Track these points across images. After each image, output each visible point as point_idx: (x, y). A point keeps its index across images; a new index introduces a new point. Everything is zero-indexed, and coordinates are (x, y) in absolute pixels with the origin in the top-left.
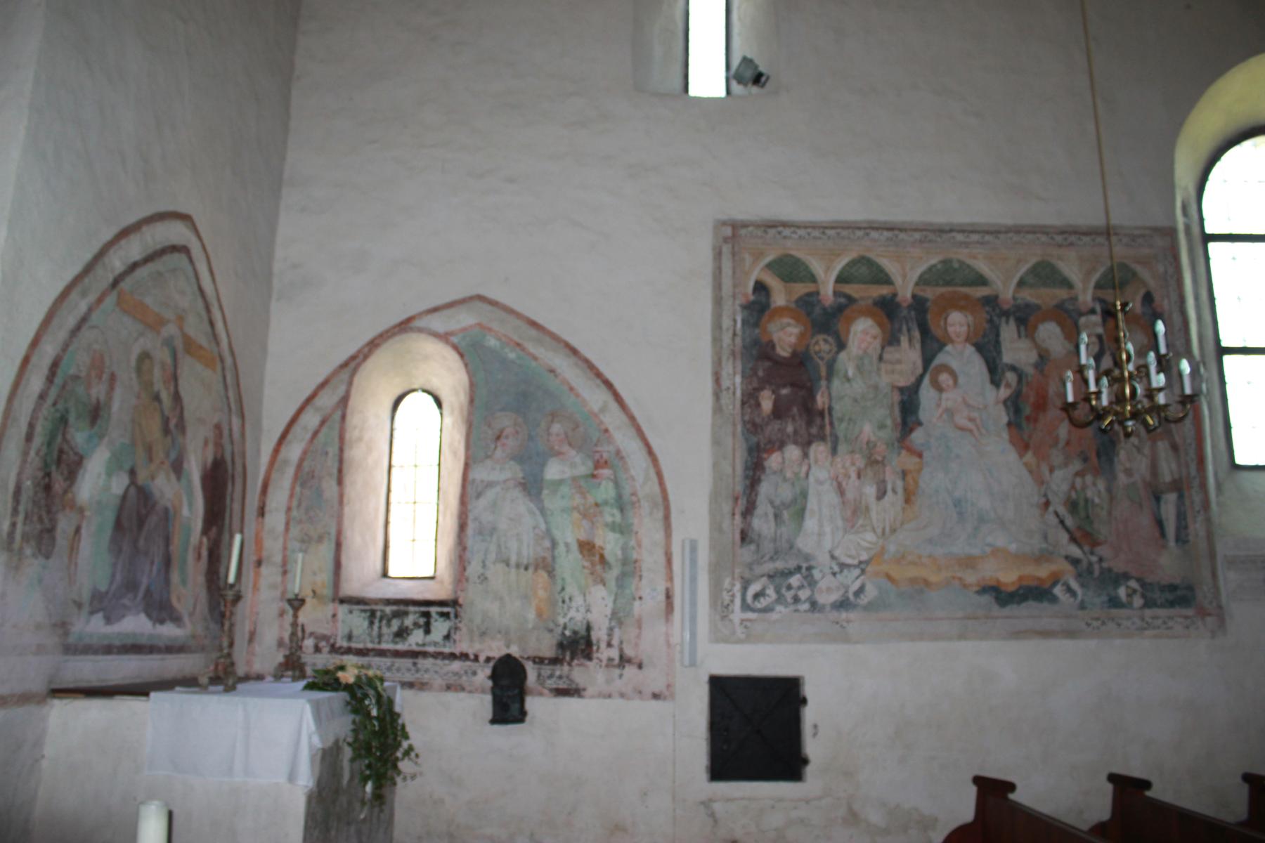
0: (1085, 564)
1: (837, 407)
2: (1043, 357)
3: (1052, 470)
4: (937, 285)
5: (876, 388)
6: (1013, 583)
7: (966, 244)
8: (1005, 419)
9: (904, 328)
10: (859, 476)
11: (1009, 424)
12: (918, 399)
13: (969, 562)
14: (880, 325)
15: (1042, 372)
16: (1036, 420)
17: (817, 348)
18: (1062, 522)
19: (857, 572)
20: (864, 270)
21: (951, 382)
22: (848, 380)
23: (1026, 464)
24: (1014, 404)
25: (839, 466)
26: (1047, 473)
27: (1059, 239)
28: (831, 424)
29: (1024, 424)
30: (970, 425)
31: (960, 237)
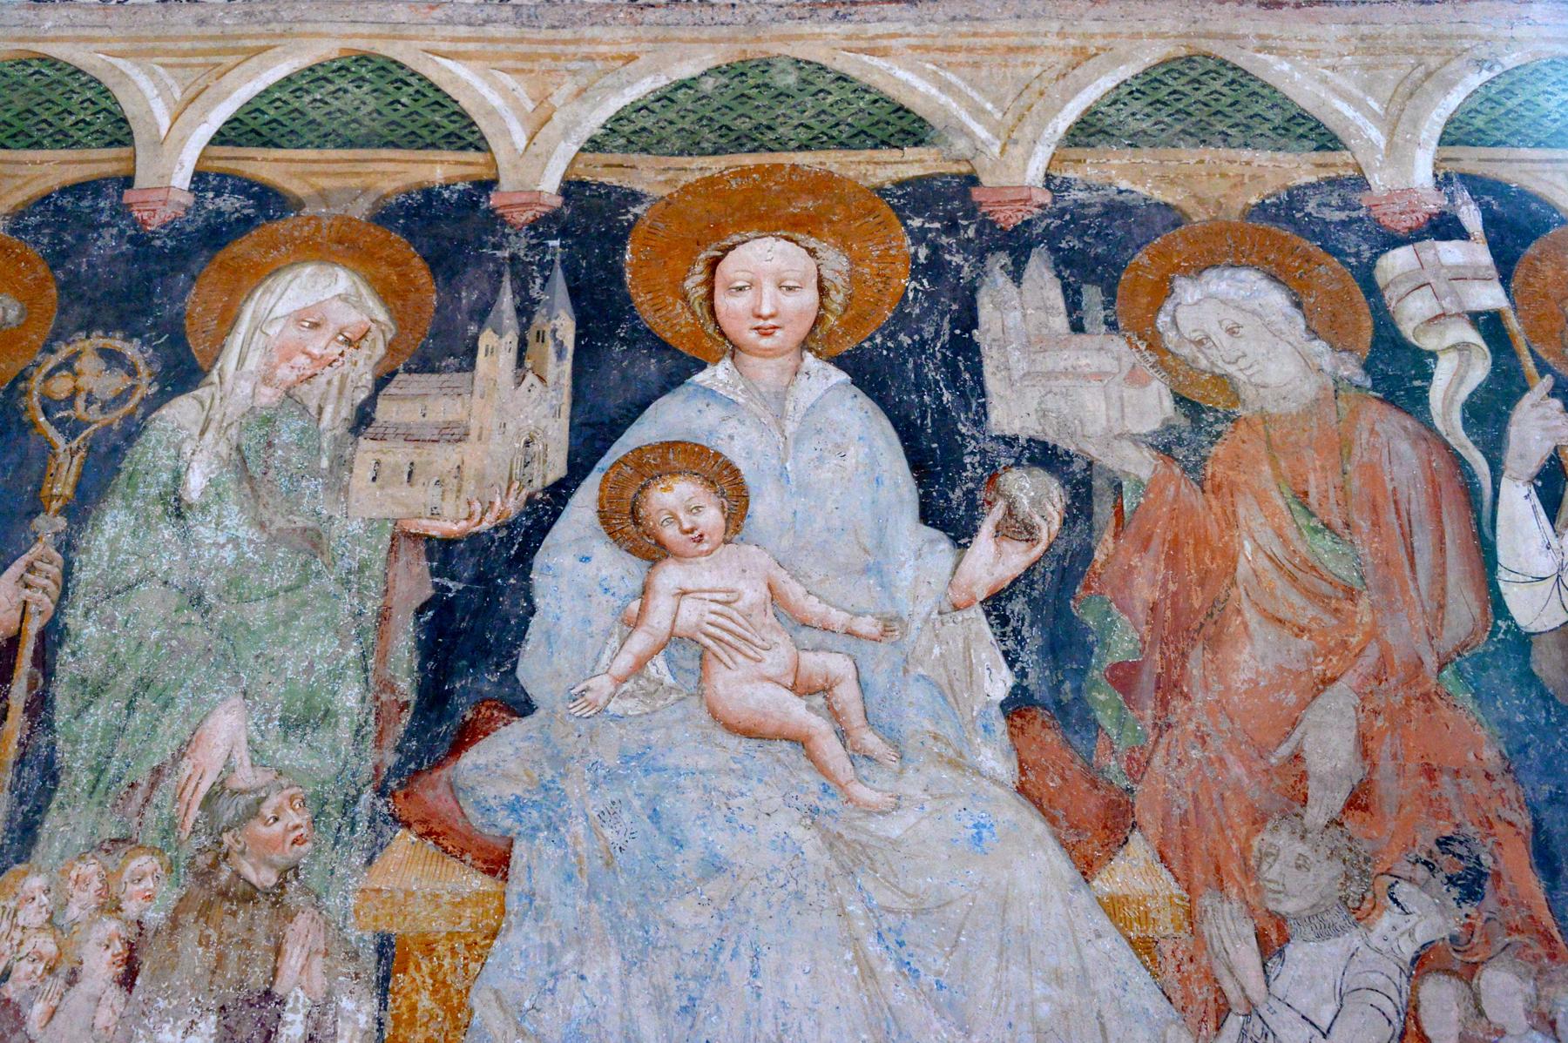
1: (86, 630)
2: (1202, 408)
4: (693, 148)
5: (314, 541)
8: (999, 684)
9: (507, 301)
10: (128, 980)
11: (1017, 706)
12: (527, 593)
14: (385, 294)
15: (1194, 470)
16: (1169, 687)
17: (61, 386)
20: (360, 101)
21: (711, 517)
22: (178, 510)
23: (1112, 907)
25: (31, 916)
26: (1247, 956)
28: (40, 706)
29: (1103, 698)
30: (798, 712)
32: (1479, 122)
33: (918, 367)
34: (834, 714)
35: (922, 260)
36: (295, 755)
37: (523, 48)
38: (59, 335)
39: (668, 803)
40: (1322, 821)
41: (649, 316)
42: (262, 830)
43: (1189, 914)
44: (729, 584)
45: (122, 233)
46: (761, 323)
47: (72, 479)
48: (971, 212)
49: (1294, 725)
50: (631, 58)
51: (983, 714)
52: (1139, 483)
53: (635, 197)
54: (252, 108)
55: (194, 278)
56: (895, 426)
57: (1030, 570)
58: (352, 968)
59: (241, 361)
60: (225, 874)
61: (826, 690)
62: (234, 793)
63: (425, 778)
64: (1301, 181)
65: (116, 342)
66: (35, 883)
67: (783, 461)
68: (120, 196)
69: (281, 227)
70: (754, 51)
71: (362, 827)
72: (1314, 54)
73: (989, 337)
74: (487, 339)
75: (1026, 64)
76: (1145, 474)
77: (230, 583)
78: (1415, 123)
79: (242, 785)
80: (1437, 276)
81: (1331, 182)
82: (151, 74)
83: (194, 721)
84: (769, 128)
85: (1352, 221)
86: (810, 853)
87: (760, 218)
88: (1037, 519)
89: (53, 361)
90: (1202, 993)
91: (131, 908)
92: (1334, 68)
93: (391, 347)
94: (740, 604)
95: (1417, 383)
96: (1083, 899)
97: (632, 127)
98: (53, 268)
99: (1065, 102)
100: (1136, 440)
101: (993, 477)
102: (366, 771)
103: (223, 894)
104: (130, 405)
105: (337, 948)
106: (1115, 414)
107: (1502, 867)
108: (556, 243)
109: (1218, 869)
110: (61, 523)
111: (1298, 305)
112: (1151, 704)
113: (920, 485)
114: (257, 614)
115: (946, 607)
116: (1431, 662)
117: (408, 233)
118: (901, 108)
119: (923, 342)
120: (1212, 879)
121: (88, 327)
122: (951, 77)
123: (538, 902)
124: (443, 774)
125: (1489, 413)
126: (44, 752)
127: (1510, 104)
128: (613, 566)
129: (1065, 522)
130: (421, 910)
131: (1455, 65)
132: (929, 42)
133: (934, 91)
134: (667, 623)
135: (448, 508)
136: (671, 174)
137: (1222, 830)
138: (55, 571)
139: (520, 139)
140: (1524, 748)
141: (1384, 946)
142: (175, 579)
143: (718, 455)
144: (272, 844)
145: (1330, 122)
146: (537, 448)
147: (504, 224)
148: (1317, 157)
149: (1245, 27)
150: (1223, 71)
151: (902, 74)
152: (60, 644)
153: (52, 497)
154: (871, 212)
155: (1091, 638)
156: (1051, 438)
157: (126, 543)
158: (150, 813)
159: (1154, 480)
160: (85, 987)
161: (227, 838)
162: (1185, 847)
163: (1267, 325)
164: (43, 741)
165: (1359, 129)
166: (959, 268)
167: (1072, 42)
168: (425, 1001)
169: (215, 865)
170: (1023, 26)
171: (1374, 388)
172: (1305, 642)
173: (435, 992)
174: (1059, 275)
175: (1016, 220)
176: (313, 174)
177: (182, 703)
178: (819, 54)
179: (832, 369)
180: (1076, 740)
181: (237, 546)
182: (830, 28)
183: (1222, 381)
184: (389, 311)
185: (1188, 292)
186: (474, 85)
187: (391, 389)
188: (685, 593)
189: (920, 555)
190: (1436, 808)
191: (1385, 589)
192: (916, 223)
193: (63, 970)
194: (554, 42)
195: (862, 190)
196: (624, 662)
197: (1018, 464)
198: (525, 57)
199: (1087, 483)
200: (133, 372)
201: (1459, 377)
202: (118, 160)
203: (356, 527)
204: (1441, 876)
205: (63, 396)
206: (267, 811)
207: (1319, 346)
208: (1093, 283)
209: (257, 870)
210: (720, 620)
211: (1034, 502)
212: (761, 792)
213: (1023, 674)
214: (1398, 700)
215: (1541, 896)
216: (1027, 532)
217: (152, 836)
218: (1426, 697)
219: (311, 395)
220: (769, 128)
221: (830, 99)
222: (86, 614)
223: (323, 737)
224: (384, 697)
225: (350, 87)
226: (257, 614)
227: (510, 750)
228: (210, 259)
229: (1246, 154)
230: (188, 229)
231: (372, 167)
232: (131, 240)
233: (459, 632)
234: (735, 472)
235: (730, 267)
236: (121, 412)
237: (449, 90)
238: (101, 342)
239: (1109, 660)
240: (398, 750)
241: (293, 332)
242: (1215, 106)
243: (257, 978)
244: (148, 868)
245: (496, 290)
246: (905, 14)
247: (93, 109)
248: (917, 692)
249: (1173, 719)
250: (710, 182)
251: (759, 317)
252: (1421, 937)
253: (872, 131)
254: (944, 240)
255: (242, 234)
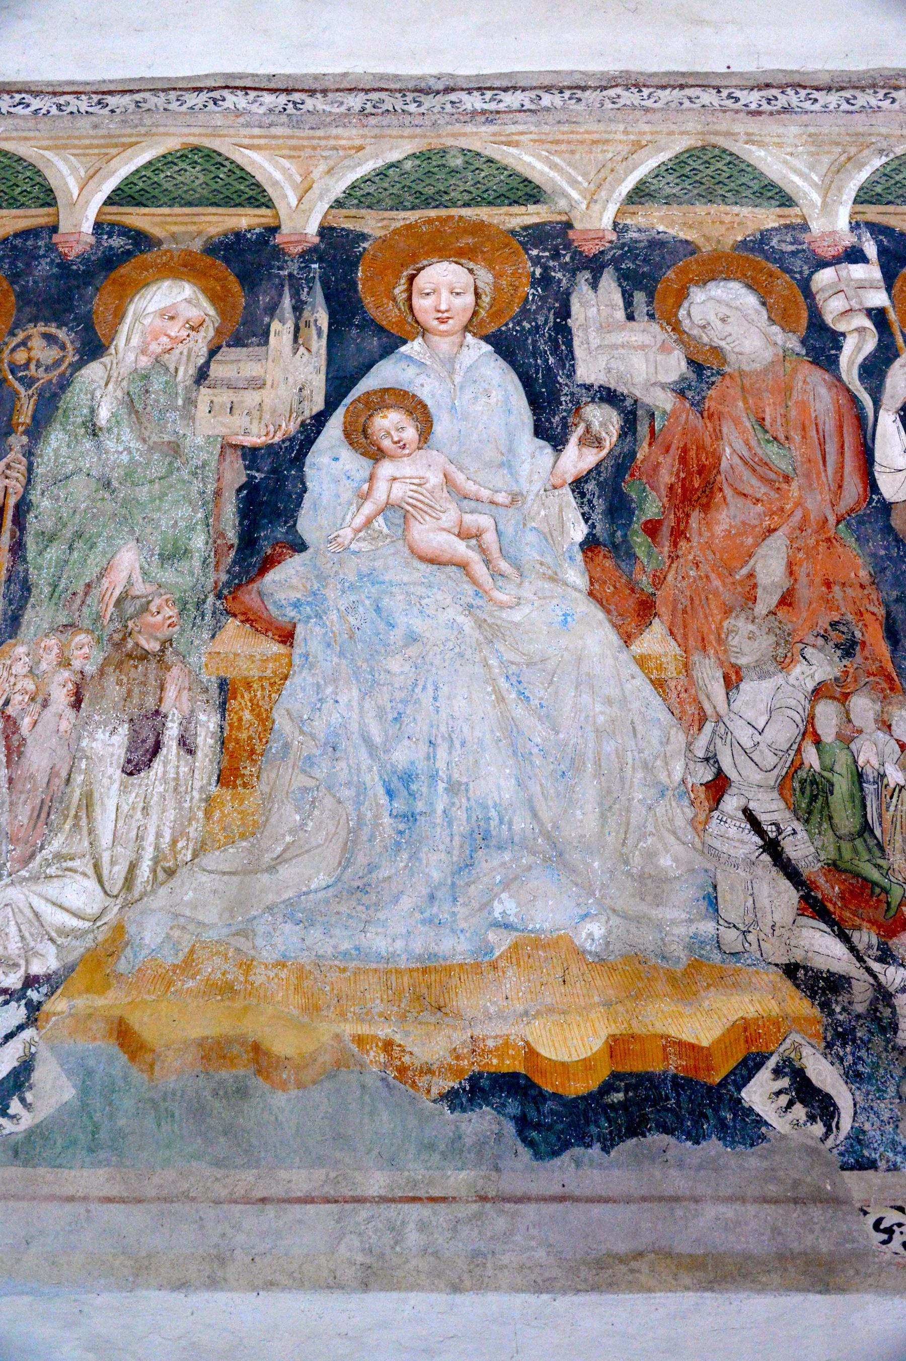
0: (861, 995)
2: (704, 367)
3: (732, 680)
4: (399, 206)
5: (175, 449)
6: (587, 1064)
7: (489, 117)
8: (579, 532)
9: (287, 302)
10: (77, 704)
11: (590, 545)
13: (427, 988)
14: (214, 298)
16: (679, 534)
17: (21, 356)
18: (772, 847)
19: (16, 1013)
20: (194, 177)
21: (410, 434)
22: (94, 431)
23: (641, 661)
24: (608, 494)
25: (20, 669)
26: (718, 689)
27: (753, 98)
29: (639, 540)
30: (461, 549)
31: (474, 102)
32: (879, 189)
33: (534, 342)
34: (482, 550)
35: (538, 276)
36: (168, 576)
37: (294, 142)
38: (17, 325)
39: (386, 602)
40: (764, 612)
41: (373, 312)
42: (151, 620)
43: (686, 665)
44: (421, 474)
45: (52, 261)
46: (440, 315)
47: (30, 413)
48: (568, 245)
49: (750, 556)
50: (361, 148)
51: (569, 550)
52: (664, 412)
53: (364, 237)
54: (128, 182)
55: (97, 289)
56: (520, 379)
57: (598, 465)
58: (204, 697)
59: (128, 340)
60: (130, 644)
61: (478, 536)
62: (133, 598)
63: (244, 589)
64: (769, 226)
65: (52, 329)
66: (21, 650)
67: (453, 400)
68: (51, 238)
69: (149, 257)
70: (436, 143)
71: (208, 617)
72: (779, 145)
73: (578, 323)
74: (275, 326)
75: (603, 151)
76: (668, 407)
77: (126, 474)
78: (840, 190)
79: (138, 593)
80: (848, 286)
81: (787, 226)
82: (66, 160)
83: (109, 556)
84: (445, 193)
85: (798, 251)
86: (467, 629)
87: (440, 250)
88: (604, 434)
89: (15, 341)
90: (691, 709)
91: (77, 664)
92: (792, 154)
93: (218, 331)
94: (427, 485)
95: (833, 352)
96: (624, 656)
97: (362, 192)
98: (12, 283)
99: (626, 176)
100: (664, 386)
101: (578, 410)
102: (210, 584)
103: (130, 656)
104: (63, 368)
105: (195, 685)
106: (652, 370)
107: (867, 638)
108: (316, 266)
109: (703, 640)
110: (25, 439)
111: (764, 304)
112: (667, 544)
113: (534, 414)
114: (143, 493)
115: (548, 487)
116: (832, 519)
117: (226, 260)
118: (526, 180)
119: (537, 327)
120: (699, 645)
121: (35, 320)
122: (557, 160)
123: (311, 659)
124: (255, 586)
125: (875, 370)
126: (22, 575)
127: (898, 178)
128: (352, 463)
129: (620, 436)
130: (243, 664)
131: (866, 152)
132: (544, 137)
133: (546, 169)
134: (384, 498)
135: (254, 429)
136: (385, 222)
137: (706, 617)
138: (23, 468)
139: (294, 202)
140: (883, 570)
141: (797, 683)
142: (94, 473)
143: (414, 396)
144: (155, 626)
145: (788, 189)
146: (306, 392)
147: (285, 254)
148: (778, 211)
149: (738, 128)
150: (724, 156)
151: (527, 158)
152: (28, 511)
153: (19, 424)
154: (507, 245)
155: (634, 505)
156: (612, 387)
157: (64, 451)
158: (85, 610)
159: (674, 411)
160: (53, 708)
161: (130, 624)
162: (685, 627)
163: (745, 316)
164: (21, 568)
165: (805, 193)
166: (560, 281)
167: (632, 137)
168: (247, 715)
169: (124, 639)
170: (601, 127)
171: (807, 355)
172: (759, 508)
173: (252, 710)
174: (620, 285)
175: (595, 251)
176: (167, 223)
177: (101, 546)
178: (477, 146)
179: (483, 344)
180: (623, 565)
181: (130, 453)
182: (483, 129)
183: (716, 351)
184: (216, 309)
185: (698, 295)
186: (264, 166)
187: (218, 357)
188: (395, 479)
189: (534, 456)
190: (830, 604)
191: (808, 476)
192: (534, 252)
193: (39, 699)
194: (313, 138)
195: (502, 232)
196: (359, 520)
197: (593, 401)
198: (294, 148)
199: (633, 413)
200: (63, 347)
201: (858, 349)
202: (49, 215)
203: (200, 440)
204: (831, 644)
205: (22, 362)
206: (153, 608)
207: (776, 329)
208: (641, 290)
209: (147, 641)
210: (416, 495)
211: (603, 424)
212: (439, 597)
213: (593, 526)
214: (811, 542)
215: (888, 654)
216: (598, 442)
217: (87, 623)
218: (829, 540)
219: (171, 360)
220: (445, 193)
221: (483, 174)
222: (43, 494)
223: (184, 565)
224: (219, 542)
225: (188, 168)
226: (143, 493)
227: (293, 572)
228: (106, 277)
229: (736, 209)
230: (93, 258)
231: (203, 218)
232: (58, 265)
233: (263, 503)
234: (425, 406)
235: (423, 281)
236: (57, 373)
237: (249, 169)
238: (43, 329)
239: (644, 519)
240: (228, 572)
241: (158, 322)
242: (719, 179)
243: (150, 703)
244: (85, 641)
245: (280, 295)
246: (529, 119)
247: (31, 183)
248: (531, 537)
249: (680, 553)
250: (409, 227)
251: (439, 311)
252: (818, 678)
253: (508, 194)
254: (551, 263)
255: (126, 261)
